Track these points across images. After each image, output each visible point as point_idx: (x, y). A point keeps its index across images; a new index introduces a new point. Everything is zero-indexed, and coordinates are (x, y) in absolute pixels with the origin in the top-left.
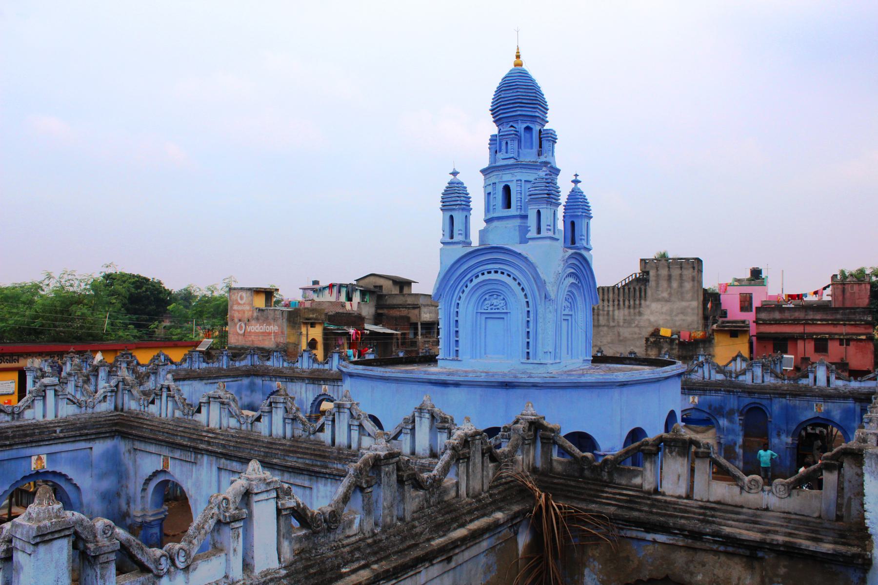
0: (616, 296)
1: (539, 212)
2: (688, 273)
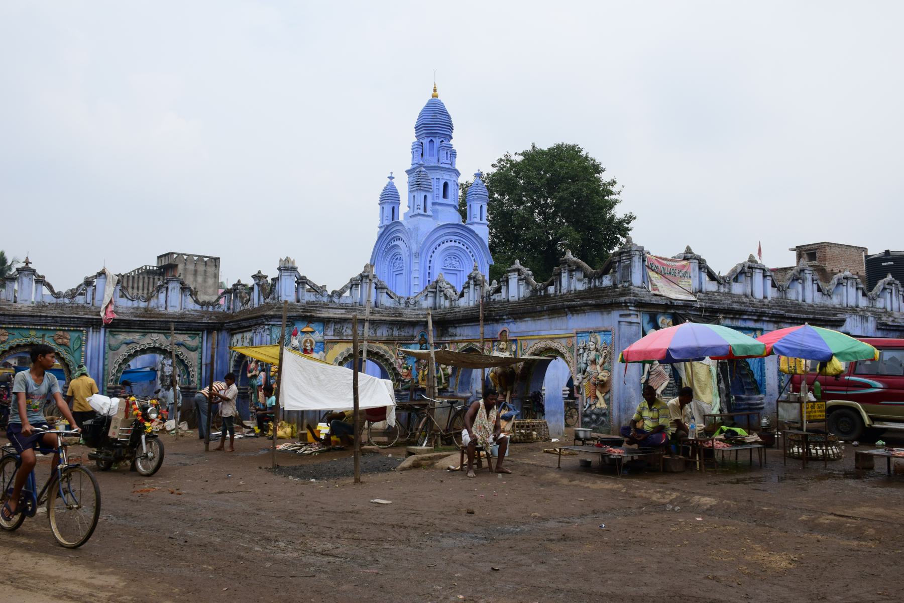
0: (146, 285)
1: (481, 206)
2: (211, 270)
